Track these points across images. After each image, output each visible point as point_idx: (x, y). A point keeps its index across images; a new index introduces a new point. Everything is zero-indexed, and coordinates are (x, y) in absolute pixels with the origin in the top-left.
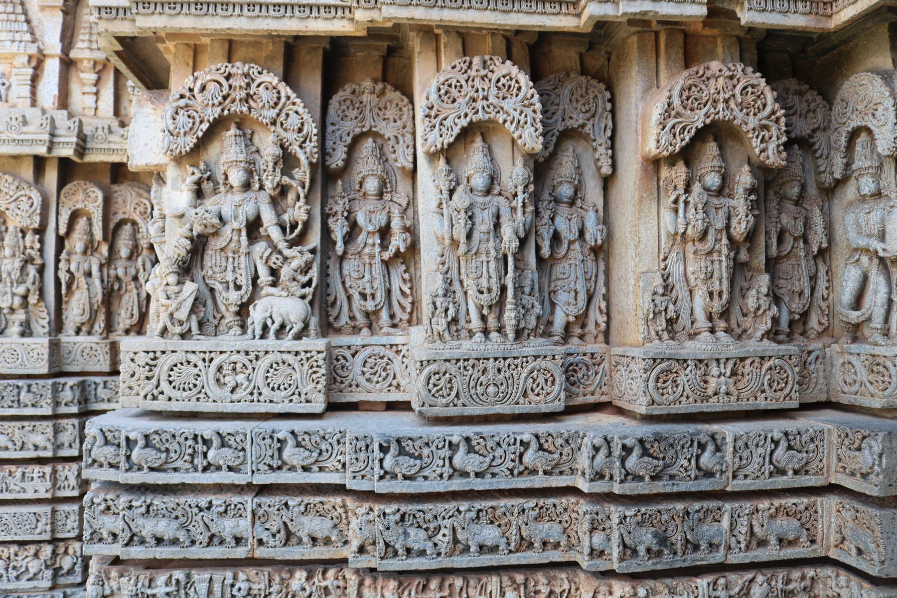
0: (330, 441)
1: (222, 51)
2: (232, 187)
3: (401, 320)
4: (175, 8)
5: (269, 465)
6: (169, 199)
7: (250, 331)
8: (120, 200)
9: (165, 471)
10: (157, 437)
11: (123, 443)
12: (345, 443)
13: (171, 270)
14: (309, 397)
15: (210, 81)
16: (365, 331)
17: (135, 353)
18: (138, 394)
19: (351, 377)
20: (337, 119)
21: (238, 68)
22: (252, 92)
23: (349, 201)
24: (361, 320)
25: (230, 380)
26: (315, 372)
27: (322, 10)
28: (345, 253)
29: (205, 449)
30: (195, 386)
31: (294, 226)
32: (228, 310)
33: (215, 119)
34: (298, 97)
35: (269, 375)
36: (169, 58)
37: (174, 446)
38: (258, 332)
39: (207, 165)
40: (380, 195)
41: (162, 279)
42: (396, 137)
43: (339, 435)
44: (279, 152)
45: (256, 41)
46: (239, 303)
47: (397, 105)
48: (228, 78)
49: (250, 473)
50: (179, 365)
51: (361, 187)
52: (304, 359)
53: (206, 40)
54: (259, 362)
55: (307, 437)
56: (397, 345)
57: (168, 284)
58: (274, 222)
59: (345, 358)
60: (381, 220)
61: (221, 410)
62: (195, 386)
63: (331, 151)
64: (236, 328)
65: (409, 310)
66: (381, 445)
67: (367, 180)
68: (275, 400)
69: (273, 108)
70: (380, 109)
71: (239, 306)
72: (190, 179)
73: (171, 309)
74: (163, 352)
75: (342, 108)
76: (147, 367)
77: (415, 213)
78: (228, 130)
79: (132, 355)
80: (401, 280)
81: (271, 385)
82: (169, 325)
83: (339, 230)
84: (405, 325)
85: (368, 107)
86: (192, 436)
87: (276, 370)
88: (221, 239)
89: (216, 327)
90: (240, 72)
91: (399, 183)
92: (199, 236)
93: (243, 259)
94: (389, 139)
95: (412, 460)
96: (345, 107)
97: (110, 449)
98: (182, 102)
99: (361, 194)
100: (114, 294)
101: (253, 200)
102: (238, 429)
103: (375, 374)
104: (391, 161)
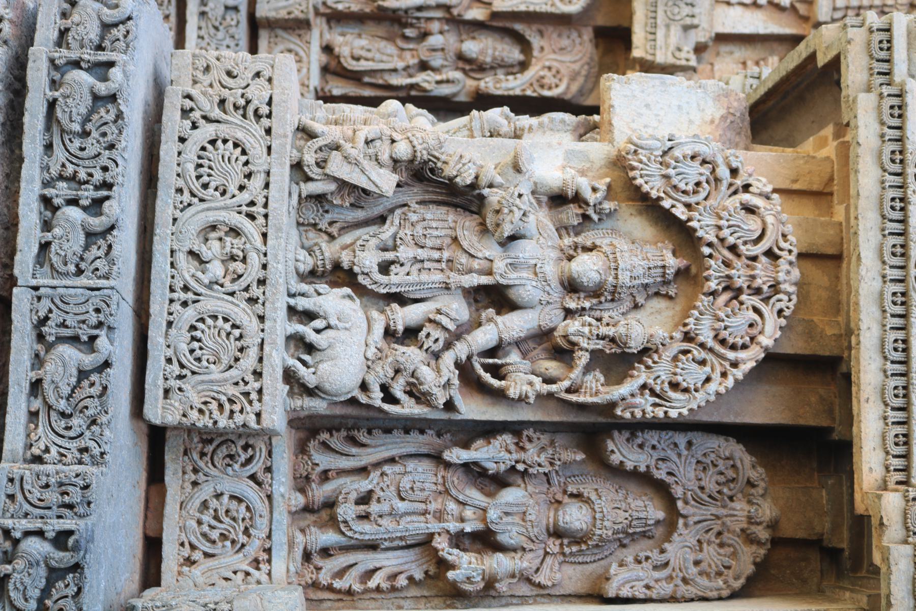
0: (88, 434)
1: (822, 242)
2: (570, 258)
3: (318, 569)
4: (893, 161)
5: (47, 318)
6: (550, 146)
7: (304, 287)
8: (565, 42)
9: (48, 128)
10: (111, 117)
11: (103, 57)
12: (80, 462)
13: (419, 148)
14: (175, 397)
15: (764, 223)
16: (299, 500)
17: (270, 80)
18: (195, 82)
19: (213, 471)
20: (700, 453)
21: (788, 274)
22: (743, 297)
23: (545, 474)
24: (320, 492)
25: (213, 249)
26: (221, 406)
27: (900, 430)
28: (448, 465)
29: (85, 202)
30: (205, 186)
31: (496, 371)
32: (344, 247)
33: (695, 230)
34: (736, 381)
36: (808, 146)
37: (92, 146)
38: (302, 303)
39: (610, 214)
40: (557, 533)
41: (404, 131)
42: (667, 564)
43: (96, 451)
44: (635, 346)
45: (839, 303)
46: (356, 269)
47: (728, 568)
48: (769, 253)
49: (34, 282)
51: (572, 496)
52: (248, 388)
53: (839, 213)
54: (244, 304)
55: (96, 390)
56: (269, 561)
57: (393, 141)
58: (506, 336)
59: (249, 461)
60: (509, 534)
61: (157, 231)
63: (639, 441)
65: (337, 584)
66: (70, 533)
67: (585, 509)
68: (173, 331)
69: (716, 336)
70: (719, 534)
71: (351, 270)
72: (584, 185)
73: (347, 146)
74: (268, 131)
75: (721, 463)
76: (242, 102)
77: (523, 600)
78: (674, 253)
79: (266, 73)
80: (396, 570)
81: (200, 325)
82: (320, 142)
83: (491, 454)
84: (309, 578)
85: (724, 512)
86: (109, 180)
87: (228, 334)
88: (475, 239)
89: (315, 225)
90: (781, 276)
91: (579, 567)
92: (482, 198)
93: (438, 277)
94: (663, 551)
95: (37, 593)
96: (721, 467)
97: (93, 32)
98: (723, 172)
99: (559, 497)
100: (396, 28)
101: (545, 298)
102: (119, 263)
103: (216, 518)
104: (621, 554)
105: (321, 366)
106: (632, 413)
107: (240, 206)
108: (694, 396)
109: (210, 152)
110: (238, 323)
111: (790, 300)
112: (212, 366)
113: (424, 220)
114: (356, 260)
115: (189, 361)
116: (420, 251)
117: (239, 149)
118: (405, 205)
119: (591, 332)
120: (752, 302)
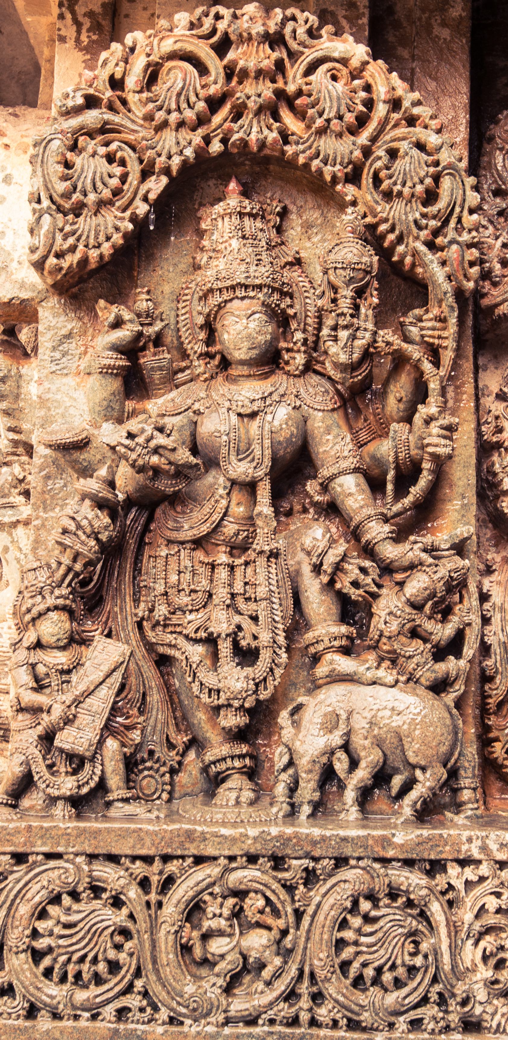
2: (225, 363)
15: (172, 56)
30: (114, 967)
33: (185, 163)
35: (349, 935)
38: (308, 790)
48: (222, 48)
50: (66, 900)
54: (316, 895)
62: (114, 967)
64: (236, 781)
68: (366, 1017)
71: (250, 712)
87: (367, 919)
90: (258, 29)
98: (92, 117)
105: (413, 759)
106: (472, 264)
107: (148, 904)
108: (445, 168)
109: (55, 960)
110: (349, 904)
111: (294, 18)
112: (424, 946)
113: (166, 594)
114: (236, 704)
115: (415, 989)
116: (216, 599)
117: (50, 908)
118: (140, 625)
119: (346, 327)
120: (298, 76)
